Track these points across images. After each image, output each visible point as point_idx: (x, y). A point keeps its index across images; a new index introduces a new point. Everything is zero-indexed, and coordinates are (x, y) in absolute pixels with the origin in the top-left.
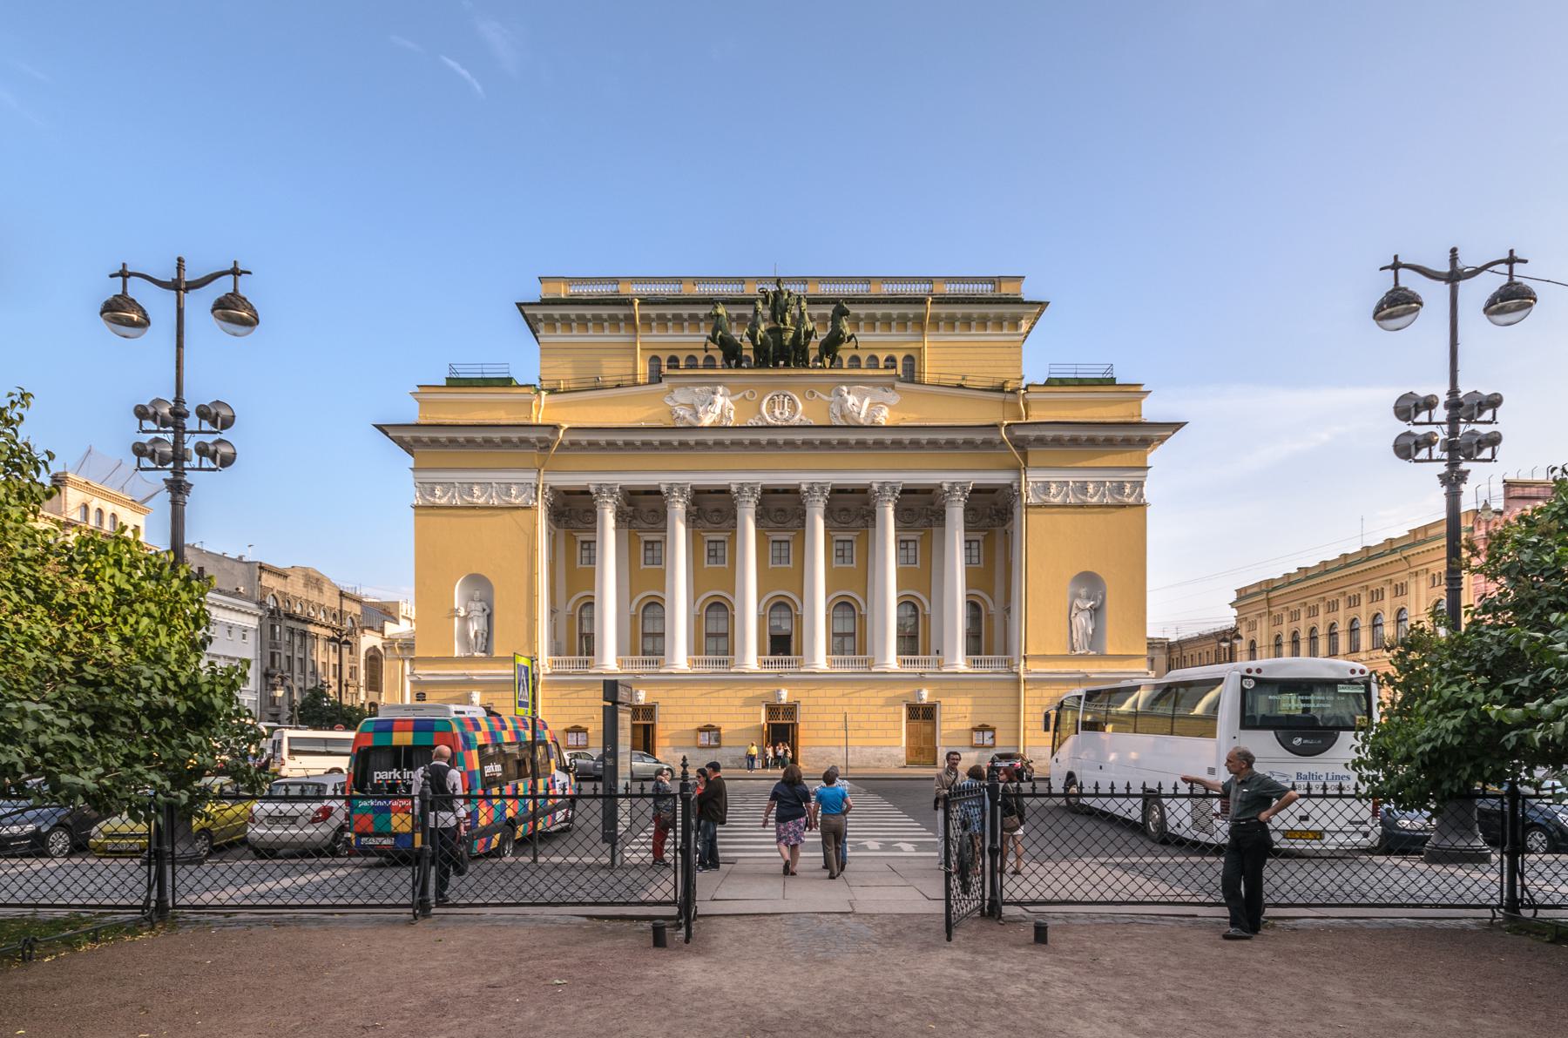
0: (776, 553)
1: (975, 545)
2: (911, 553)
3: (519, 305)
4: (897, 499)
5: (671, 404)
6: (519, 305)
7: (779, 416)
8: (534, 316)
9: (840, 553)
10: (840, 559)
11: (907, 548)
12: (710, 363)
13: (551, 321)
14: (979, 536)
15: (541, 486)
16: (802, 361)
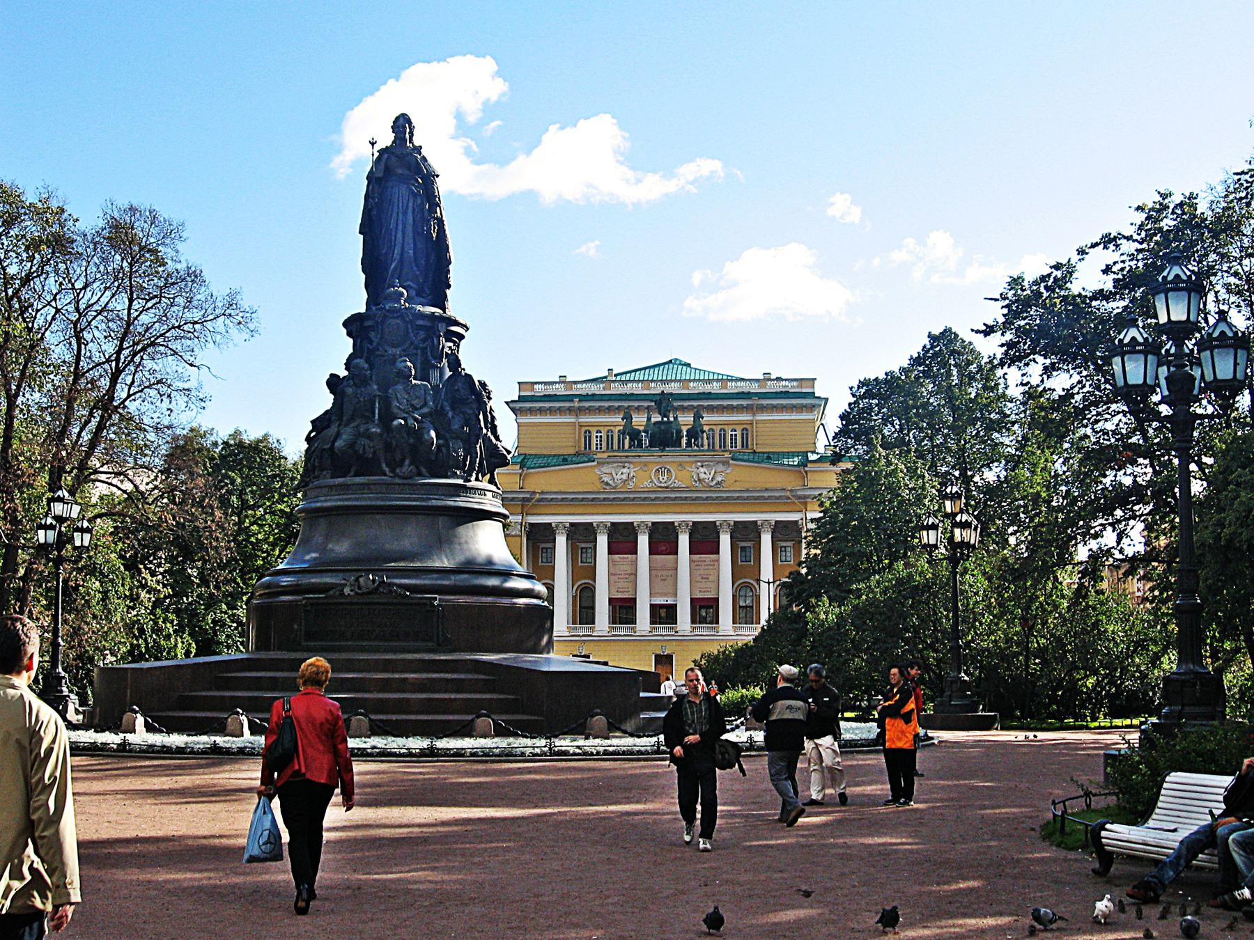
1: (788, 549)
3: (507, 403)
6: (507, 403)
12: (621, 448)
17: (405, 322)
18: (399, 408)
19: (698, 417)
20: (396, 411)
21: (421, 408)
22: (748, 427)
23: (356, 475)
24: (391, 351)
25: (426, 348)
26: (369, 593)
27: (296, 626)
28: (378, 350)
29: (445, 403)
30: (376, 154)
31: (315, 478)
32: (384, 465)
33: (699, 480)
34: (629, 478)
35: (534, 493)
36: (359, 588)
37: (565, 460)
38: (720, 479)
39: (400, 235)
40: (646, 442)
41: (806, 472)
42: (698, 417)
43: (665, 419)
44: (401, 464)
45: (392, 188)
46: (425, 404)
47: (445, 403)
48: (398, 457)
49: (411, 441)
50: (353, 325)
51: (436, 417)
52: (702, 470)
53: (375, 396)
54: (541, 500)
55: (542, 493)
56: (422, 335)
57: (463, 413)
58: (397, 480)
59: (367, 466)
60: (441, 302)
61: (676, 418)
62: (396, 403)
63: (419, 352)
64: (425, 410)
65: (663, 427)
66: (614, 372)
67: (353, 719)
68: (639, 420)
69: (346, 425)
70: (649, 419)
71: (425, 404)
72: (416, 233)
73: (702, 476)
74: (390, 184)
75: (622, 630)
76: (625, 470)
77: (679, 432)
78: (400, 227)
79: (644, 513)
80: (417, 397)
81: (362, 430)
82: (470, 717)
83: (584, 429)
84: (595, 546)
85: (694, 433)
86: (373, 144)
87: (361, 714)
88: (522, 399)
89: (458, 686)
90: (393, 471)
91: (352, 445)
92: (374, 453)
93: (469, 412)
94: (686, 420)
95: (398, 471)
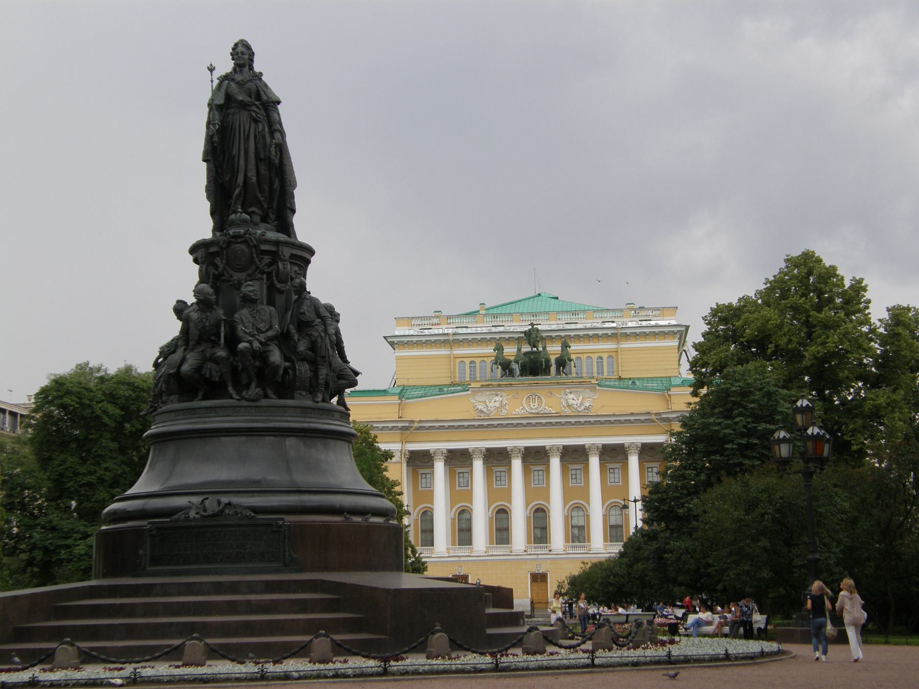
0: (536, 478)
3: (385, 337)
4: (600, 452)
6: (385, 337)
7: (534, 407)
8: (393, 342)
9: (574, 477)
10: (574, 481)
11: (614, 473)
15: (403, 451)
16: (547, 371)
17: (249, 246)
18: (246, 332)
19: (565, 346)
20: (241, 334)
21: (267, 330)
23: (205, 398)
24: (236, 276)
25: (271, 273)
26: (214, 515)
27: (141, 552)
28: (223, 275)
29: (291, 327)
30: (216, 82)
31: (163, 403)
32: (231, 389)
33: (568, 406)
34: (502, 406)
35: (413, 422)
36: (205, 511)
37: (441, 389)
38: (587, 404)
39: (242, 162)
41: (670, 396)
42: (565, 346)
43: (535, 349)
44: (247, 386)
45: (233, 114)
46: (271, 327)
47: (291, 327)
48: (244, 379)
49: (257, 364)
50: (200, 251)
51: (283, 339)
52: (570, 396)
53: (220, 320)
54: (417, 429)
55: (420, 421)
56: (267, 259)
57: (310, 335)
58: (244, 403)
59: (215, 389)
60: (286, 227)
61: (544, 348)
62: (240, 327)
63: (265, 276)
64: (270, 333)
65: (532, 357)
66: (487, 306)
67: (187, 643)
68: (510, 351)
69: (192, 350)
70: (519, 350)
71: (271, 327)
72: (258, 159)
73: (571, 402)
74: (231, 111)
75: (500, 550)
76: (497, 398)
77: (548, 361)
78: (242, 153)
79: (517, 439)
80: (263, 321)
81: (208, 355)
82: (306, 638)
83: (458, 360)
84: (472, 470)
85: (562, 363)
86: (211, 69)
87: (196, 639)
89: (303, 606)
90: (239, 393)
91: (198, 369)
92: (221, 377)
93: (316, 334)
94: (554, 350)
95: (244, 393)
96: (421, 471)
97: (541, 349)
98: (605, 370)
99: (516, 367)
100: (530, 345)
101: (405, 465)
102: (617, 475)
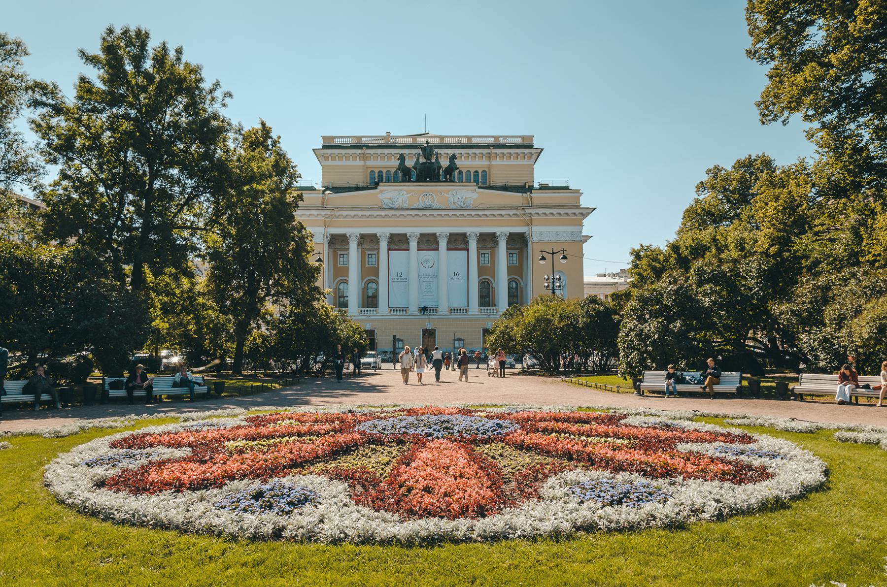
1: (515, 255)
2: (486, 259)
3: (314, 150)
5: (381, 198)
6: (314, 150)
13: (326, 158)
14: (516, 251)
19: (453, 158)
22: (487, 170)
37: (357, 189)
40: (414, 178)
42: (453, 158)
68: (410, 163)
77: (440, 167)
88: (325, 147)
94: (445, 163)
96: (339, 252)
97: (433, 160)
98: (480, 180)
99: (414, 173)
100: (425, 157)
101: (326, 245)
102: (486, 259)
